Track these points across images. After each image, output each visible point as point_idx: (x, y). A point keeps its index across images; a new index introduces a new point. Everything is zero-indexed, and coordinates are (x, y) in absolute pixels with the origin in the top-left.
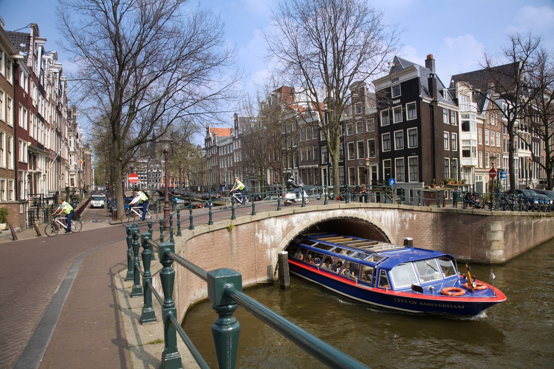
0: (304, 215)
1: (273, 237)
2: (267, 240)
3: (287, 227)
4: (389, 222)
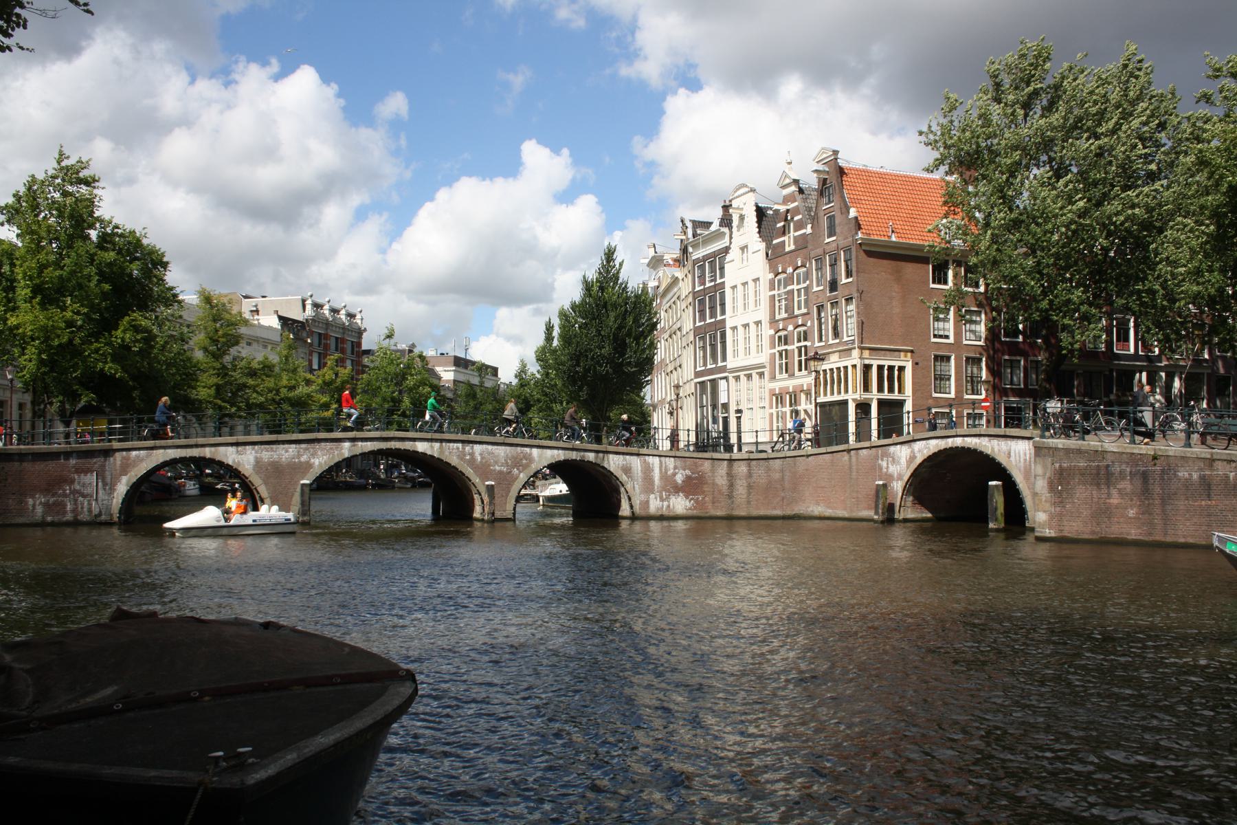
0: (924, 442)
2: (893, 470)
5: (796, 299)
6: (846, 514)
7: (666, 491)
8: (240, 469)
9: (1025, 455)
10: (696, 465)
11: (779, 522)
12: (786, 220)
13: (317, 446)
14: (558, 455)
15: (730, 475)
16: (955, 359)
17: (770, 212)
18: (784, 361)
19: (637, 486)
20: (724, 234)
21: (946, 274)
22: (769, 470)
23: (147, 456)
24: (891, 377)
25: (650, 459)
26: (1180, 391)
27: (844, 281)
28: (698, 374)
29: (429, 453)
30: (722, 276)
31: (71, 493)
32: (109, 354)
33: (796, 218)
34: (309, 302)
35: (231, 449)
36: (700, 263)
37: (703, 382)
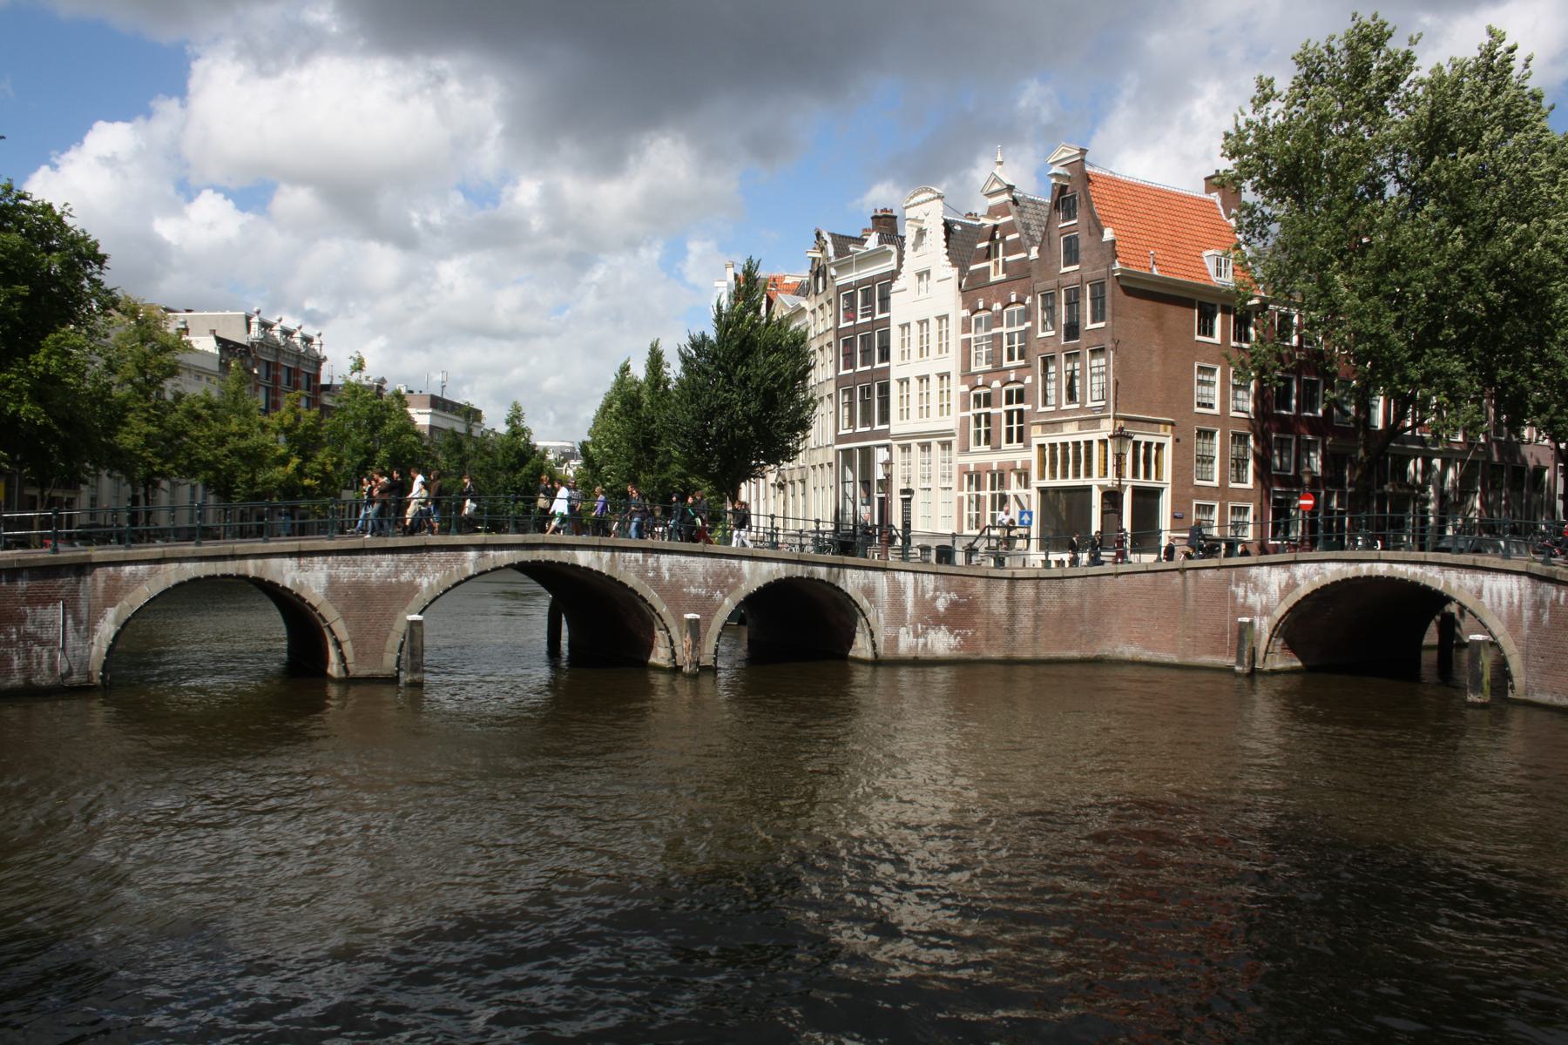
1: (1264, 598)
2: (1254, 600)
3: (1287, 585)
4: (1504, 602)
5: (1005, 346)
6: (1174, 658)
7: (922, 623)
8: (303, 595)
9: (1511, 595)
10: (964, 585)
11: (1073, 671)
12: (992, 238)
13: (426, 556)
14: (778, 571)
15: (1011, 600)
16: (1221, 435)
17: (958, 228)
18: (983, 428)
19: (881, 616)
20: (890, 253)
21: (1212, 323)
22: (1064, 593)
23: (150, 574)
24: (1147, 457)
25: (901, 576)
26: (1454, 482)
27: (1090, 326)
28: (840, 439)
29: (595, 567)
30: (885, 307)
31: (19, 639)
32: (26, 389)
33: (1008, 238)
34: (255, 320)
35: (289, 563)
36: (848, 292)
37: (850, 450)
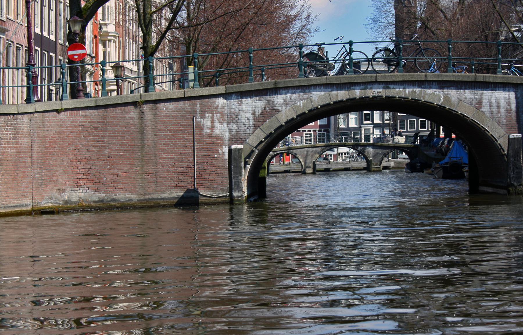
1: (234, 127)
3: (264, 111)
4: (503, 110)
6: (134, 197)
9: (509, 104)
